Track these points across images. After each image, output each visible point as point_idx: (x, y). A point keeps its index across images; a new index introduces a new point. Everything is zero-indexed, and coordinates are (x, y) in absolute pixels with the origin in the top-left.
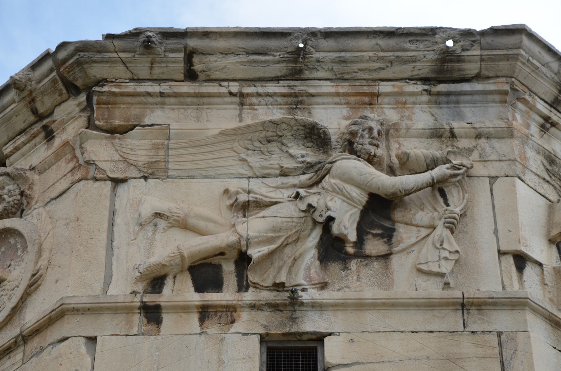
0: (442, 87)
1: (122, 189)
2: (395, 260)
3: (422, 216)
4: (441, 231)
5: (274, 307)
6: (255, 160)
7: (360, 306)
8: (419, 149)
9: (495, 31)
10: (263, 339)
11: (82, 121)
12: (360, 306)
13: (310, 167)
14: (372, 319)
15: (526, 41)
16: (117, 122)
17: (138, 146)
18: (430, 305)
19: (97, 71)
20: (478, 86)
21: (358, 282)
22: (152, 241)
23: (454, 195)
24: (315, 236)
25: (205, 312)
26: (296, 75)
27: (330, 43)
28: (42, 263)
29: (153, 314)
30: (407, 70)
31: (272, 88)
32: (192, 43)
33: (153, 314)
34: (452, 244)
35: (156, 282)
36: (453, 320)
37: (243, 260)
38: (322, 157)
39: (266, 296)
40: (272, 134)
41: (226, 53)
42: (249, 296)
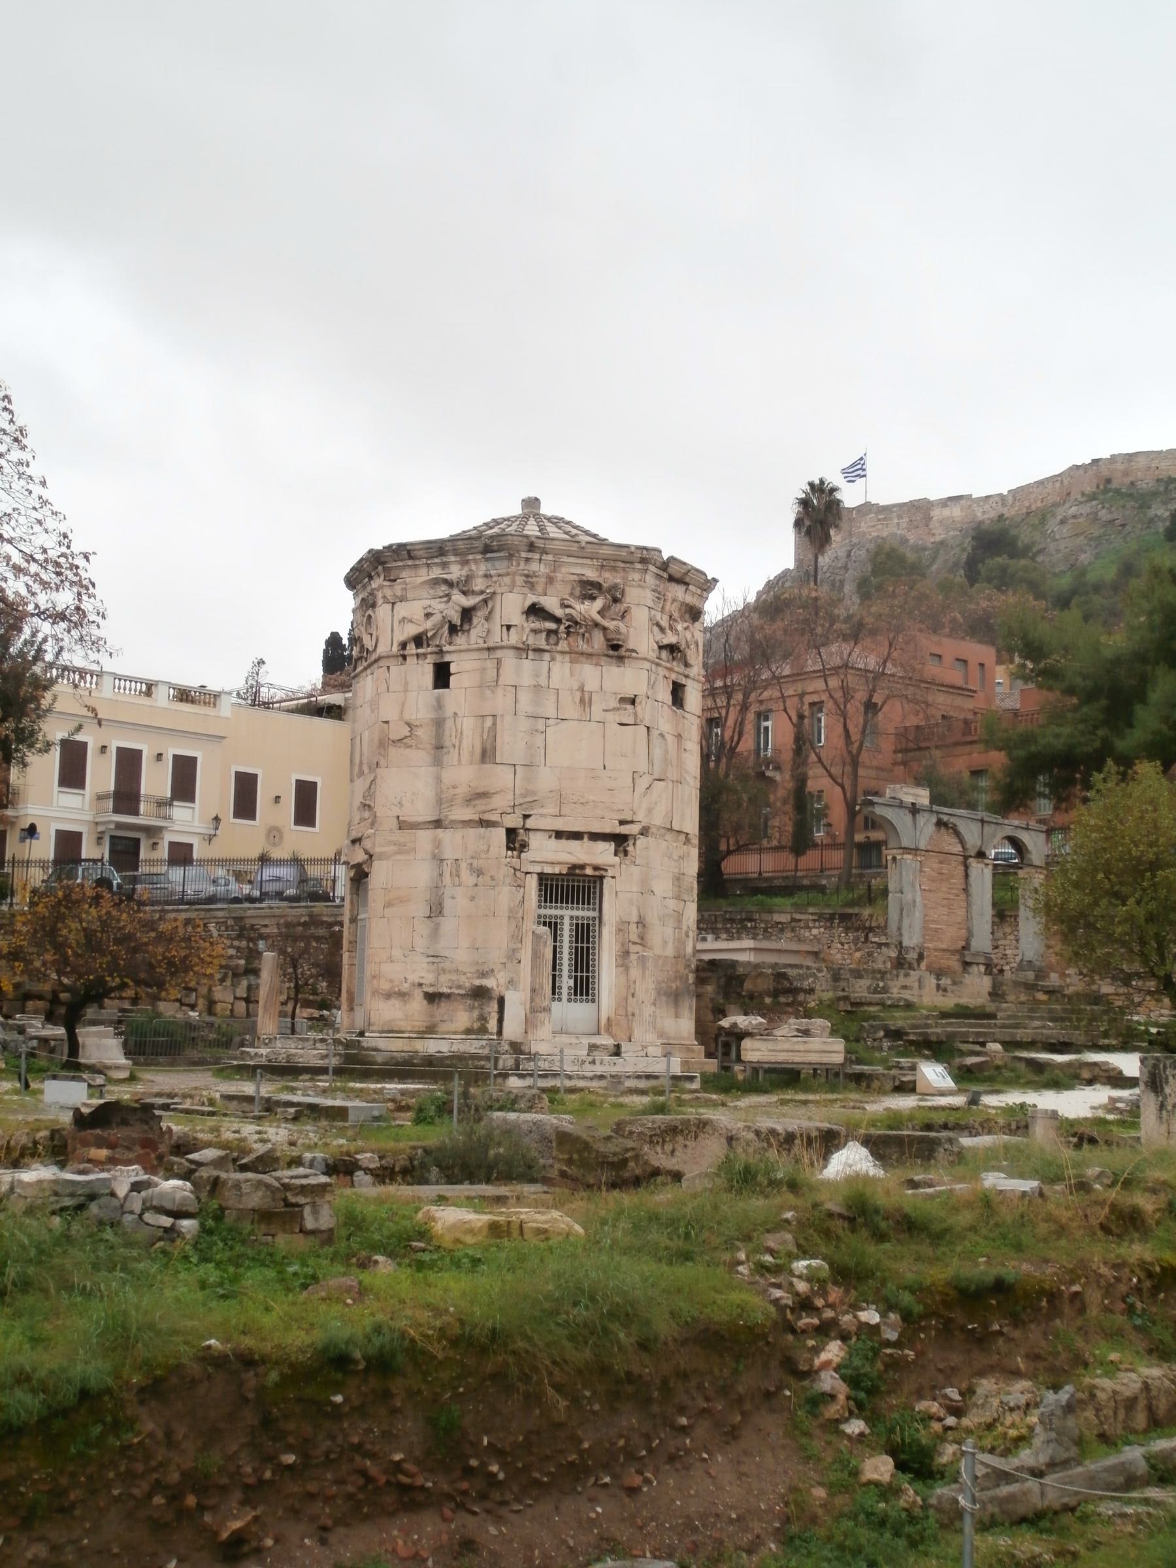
0: (489, 555)
2: (472, 631)
3: (479, 614)
6: (431, 592)
7: (460, 651)
10: (435, 664)
12: (460, 651)
14: (465, 656)
17: (398, 588)
19: (383, 559)
20: (499, 554)
21: (460, 640)
23: (490, 604)
24: (446, 627)
26: (442, 555)
31: (436, 560)
33: (404, 657)
34: (486, 626)
36: (485, 654)
39: (435, 649)
40: (436, 582)
42: (429, 650)
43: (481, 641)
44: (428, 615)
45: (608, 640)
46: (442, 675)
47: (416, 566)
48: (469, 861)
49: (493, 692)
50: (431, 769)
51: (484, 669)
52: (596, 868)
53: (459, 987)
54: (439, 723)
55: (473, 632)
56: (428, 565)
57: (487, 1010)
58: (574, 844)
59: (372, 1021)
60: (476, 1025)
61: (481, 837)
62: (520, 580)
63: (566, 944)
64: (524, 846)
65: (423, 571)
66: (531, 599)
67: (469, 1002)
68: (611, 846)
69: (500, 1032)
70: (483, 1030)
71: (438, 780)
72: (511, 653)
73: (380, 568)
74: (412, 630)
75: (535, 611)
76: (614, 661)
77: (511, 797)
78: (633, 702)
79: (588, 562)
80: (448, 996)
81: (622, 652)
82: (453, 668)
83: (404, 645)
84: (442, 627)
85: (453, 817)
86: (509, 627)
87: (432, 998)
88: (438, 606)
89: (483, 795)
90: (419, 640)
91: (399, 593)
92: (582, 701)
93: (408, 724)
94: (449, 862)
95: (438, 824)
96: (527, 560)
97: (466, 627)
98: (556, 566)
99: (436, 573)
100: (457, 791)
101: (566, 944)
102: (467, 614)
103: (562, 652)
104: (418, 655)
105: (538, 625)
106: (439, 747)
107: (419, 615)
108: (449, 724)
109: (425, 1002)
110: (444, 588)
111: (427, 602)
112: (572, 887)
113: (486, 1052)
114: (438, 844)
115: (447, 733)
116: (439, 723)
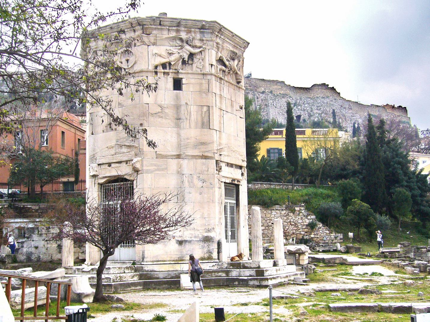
0: (202, 30)
1: (149, 47)
3: (198, 57)
4: (201, 60)
5: (175, 73)
6: (171, 43)
7: (188, 73)
8: (198, 44)
9: (211, 22)
11: (141, 31)
12: (188, 73)
13: (180, 46)
14: (190, 76)
15: (216, 24)
16: (148, 33)
17: (152, 38)
18: (199, 74)
19: (144, 23)
20: (208, 31)
21: (188, 69)
22: (155, 59)
23: (203, 53)
25: (164, 73)
26: (178, 26)
27: (184, 21)
28: (137, 59)
29: (156, 73)
30: (196, 27)
31: (174, 28)
32: (161, 19)
33: (156, 73)
34: (202, 63)
36: (201, 77)
37: (170, 64)
38: (182, 44)
39: (174, 71)
40: (174, 39)
41: (167, 21)
42: (171, 71)
43: (199, 70)
44: (171, 54)
45: (237, 79)
46: (178, 85)
48: (198, 175)
49: (207, 95)
50: (175, 129)
51: (201, 84)
52: (238, 181)
53: (195, 237)
54: (177, 107)
55: (194, 65)
57: (211, 248)
58: (230, 168)
59: (146, 256)
60: (206, 256)
61: (203, 164)
62: (215, 44)
63: (229, 216)
64: (221, 169)
65: (165, 32)
66: (220, 55)
67: (202, 244)
68: (239, 171)
69: (218, 259)
70: (210, 258)
71: (179, 135)
72: (214, 78)
73: (138, 28)
74: (164, 61)
75: (221, 61)
76: (238, 89)
77: (216, 146)
78: (241, 108)
79: (231, 43)
80: (190, 242)
82: (184, 81)
83: (156, 67)
84: (179, 60)
85: (187, 154)
86: (212, 65)
87: (180, 243)
88: (174, 50)
90: (164, 66)
91: (152, 41)
92: (231, 105)
93: (159, 106)
94: (187, 176)
95: (178, 156)
97: (190, 62)
99: (173, 34)
100: (189, 141)
101: (229, 216)
103: (226, 81)
104: (164, 73)
105: (220, 67)
107: (164, 53)
108: (183, 108)
109: (177, 246)
110: (179, 43)
111: (168, 48)
113: (215, 268)
114: (180, 166)
115: (182, 112)
116: (177, 107)
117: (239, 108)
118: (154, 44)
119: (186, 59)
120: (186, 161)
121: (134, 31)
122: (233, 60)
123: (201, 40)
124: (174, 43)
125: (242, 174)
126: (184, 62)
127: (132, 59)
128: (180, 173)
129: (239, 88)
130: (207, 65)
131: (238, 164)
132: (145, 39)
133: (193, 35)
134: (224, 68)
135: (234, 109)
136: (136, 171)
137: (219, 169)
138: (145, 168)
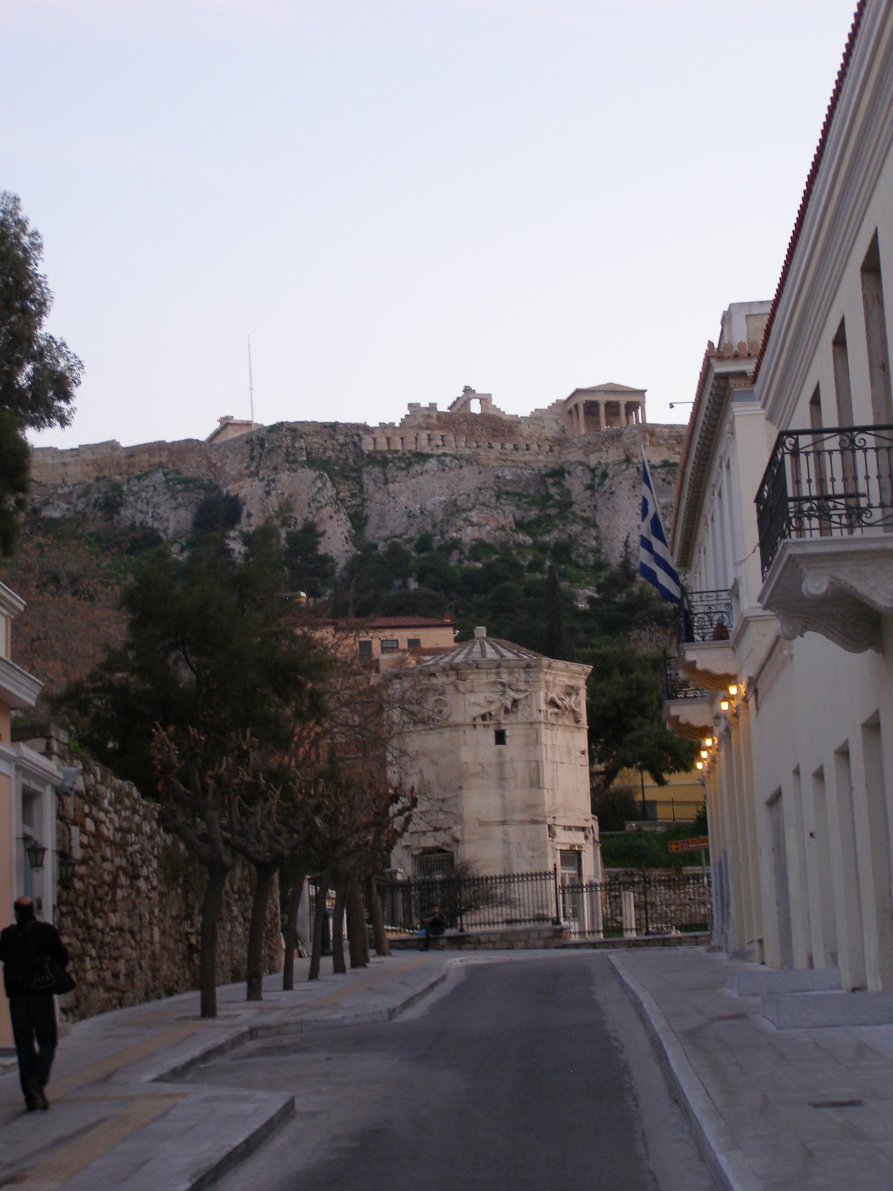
3: (523, 702)
7: (512, 724)
8: (523, 687)
12: (512, 724)
14: (514, 727)
17: (468, 684)
18: (524, 723)
21: (512, 718)
25: (484, 726)
29: (475, 726)
33: (475, 726)
35: (475, 719)
36: (528, 726)
37: (490, 714)
40: (495, 683)
44: (491, 703)
45: (575, 718)
46: (500, 738)
47: (479, 673)
52: (580, 846)
55: (519, 713)
56: (488, 673)
58: (570, 832)
62: (543, 684)
65: (484, 676)
66: (550, 695)
71: (503, 796)
72: (543, 726)
73: (451, 673)
74: (483, 711)
75: (553, 703)
81: (580, 725)
82: (507, 733)
86: (540, 711)
88: (495, 697)
89: (534, 806)
90: (484, 717)
91: (469, 688)
95: (504, 823)
96: (546, 673)
98: (555, 675)
99: (493, 678)
102: (515, 702)
105: (551, 710)
106: (502, 778)
107: (483, 702)
110: (500, 687)
111: (487, 695)
112: (572, 857)
114: (506, 834)
116: (501, 765)
117: (579, 754)
118: (471, 691)
119: (510, 707)
120: (513, 828)
121: (447, 676)
122: (569, 695)
123: (527, 682)
124: (495, 689)
125: (586, 838)
126: (507, 711)
127: (445, 710)
128: (506, 842)
129: (579, 728)
130: (535, 712)
131: (578, 825)
132: (461, 688)
133: (516, 675)
134: (556, 710)
135: (573, 756)
136: (457, 841)
137: (552, 834)
138: (466, 837)
